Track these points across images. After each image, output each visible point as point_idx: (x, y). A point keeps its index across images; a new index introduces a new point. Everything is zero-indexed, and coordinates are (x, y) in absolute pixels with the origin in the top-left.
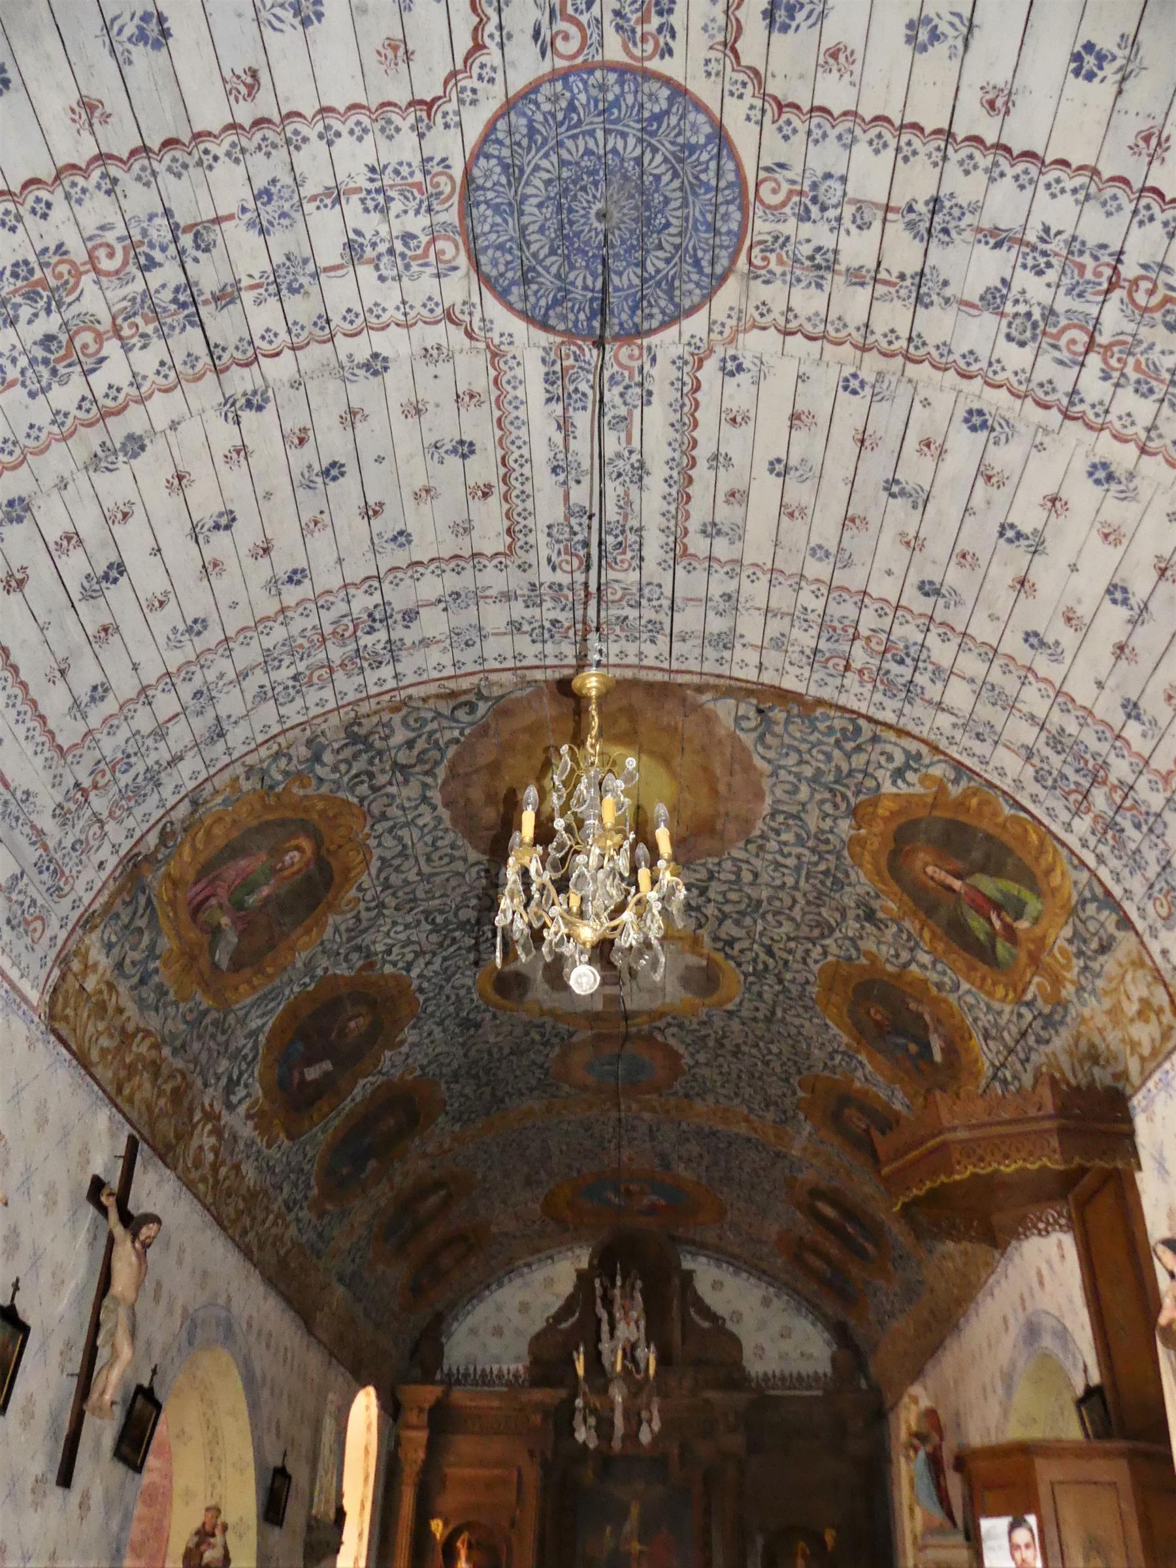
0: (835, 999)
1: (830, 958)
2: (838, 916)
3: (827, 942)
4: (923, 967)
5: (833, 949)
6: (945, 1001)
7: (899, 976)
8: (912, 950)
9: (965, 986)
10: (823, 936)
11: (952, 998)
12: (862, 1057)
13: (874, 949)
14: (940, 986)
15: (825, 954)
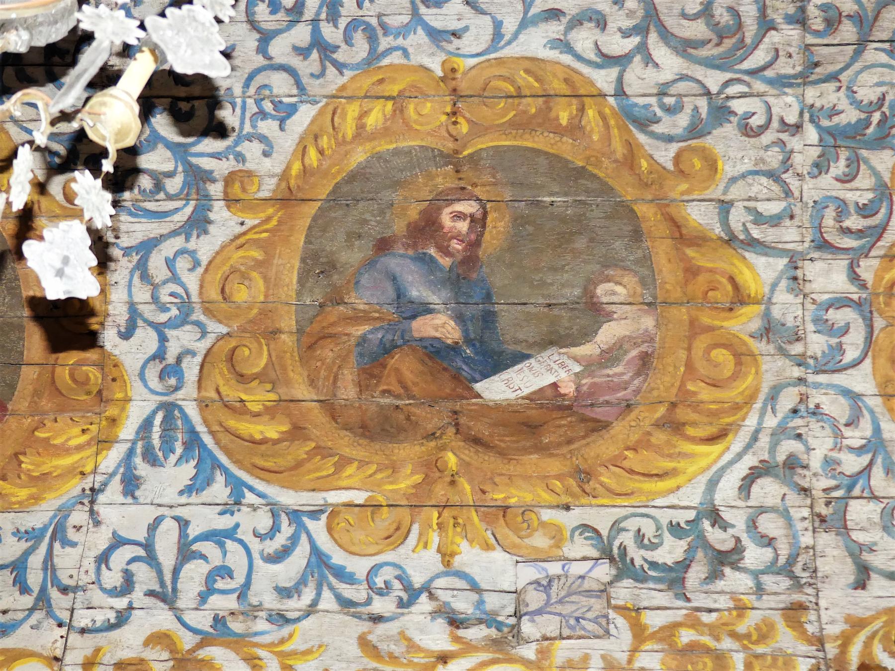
0: (429, 113)
1: (604, 79)
2: (785, 67)
3: (660, 52)
4: (796, 282)
5: (640, 80)
6: (742, 357)
7: (682, 235)
8: (823, 245)
9: (861, 380)
10: (684, 47)
11: (773, 368)
12: (225, 223)
13: (727, 169)
14: (769, 330)
15: (607, 60)
